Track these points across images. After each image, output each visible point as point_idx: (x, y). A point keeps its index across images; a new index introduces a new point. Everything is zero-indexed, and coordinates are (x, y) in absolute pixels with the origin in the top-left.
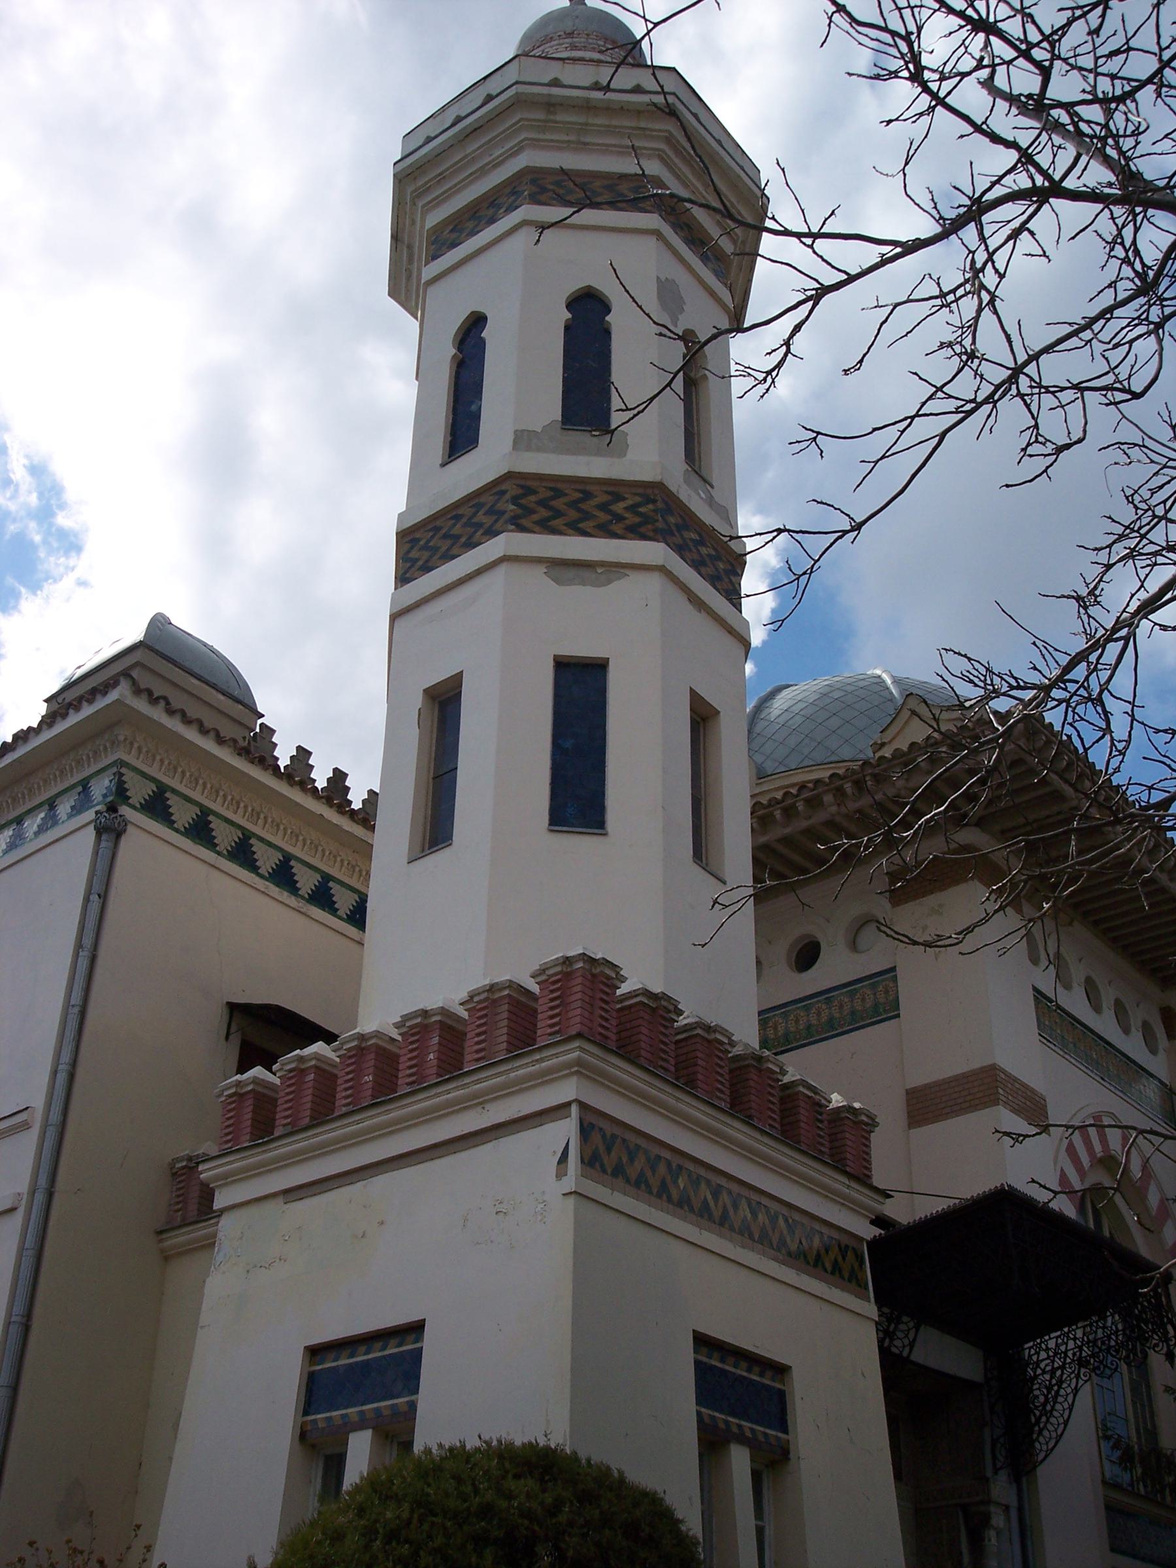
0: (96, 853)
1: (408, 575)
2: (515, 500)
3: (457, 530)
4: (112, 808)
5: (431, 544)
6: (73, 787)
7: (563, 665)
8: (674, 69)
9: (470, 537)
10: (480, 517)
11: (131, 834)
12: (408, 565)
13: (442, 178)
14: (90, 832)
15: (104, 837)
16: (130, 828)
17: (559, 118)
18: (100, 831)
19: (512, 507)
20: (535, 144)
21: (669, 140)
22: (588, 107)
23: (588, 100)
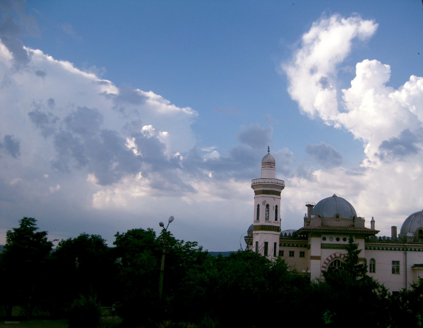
7: (275, 243)
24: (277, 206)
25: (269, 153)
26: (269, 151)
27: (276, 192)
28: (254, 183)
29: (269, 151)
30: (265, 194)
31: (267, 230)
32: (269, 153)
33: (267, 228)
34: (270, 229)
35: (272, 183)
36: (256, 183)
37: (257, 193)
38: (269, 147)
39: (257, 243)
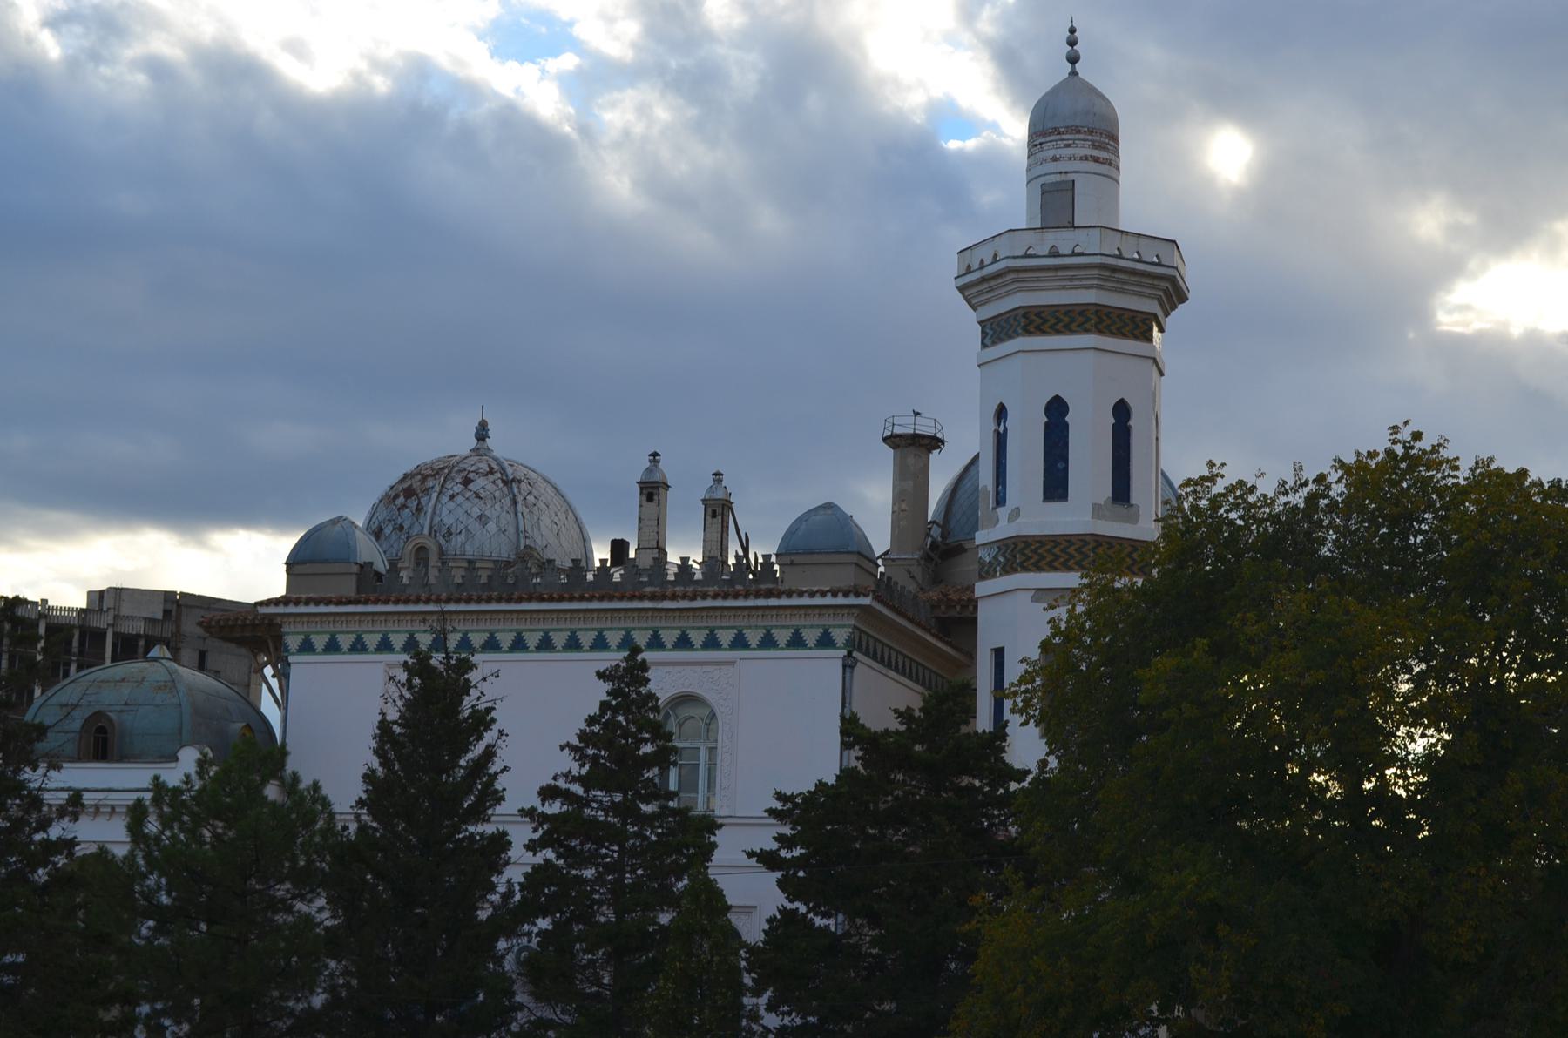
0: (844, 678)
1: (1025, 564)
2: (1093, 550)
3: (1056, 551)
4: (850, 654)
5: (1040, 551)
6: (818, 626)
8: (1175, 242)
9: (1068, 560)
10: (1071, 550)
11: (859, 668)
12: (1024, 558)
13: (1038, 280)
14: (840, 662)
15: (848, 670)
16: (859, 664)
17: (1116, 276)
18: (844, 667)
19: (1092, 554)
20: (1100, 288)
21: (1166, 292)
22: (1134, 272)
23: (1134, 269)
24: (1122, 411)
25: (1074, 73)
26: (1073, 59)
27: (1119, 316)
28: (969, 270)
29: (1073, 59)
30: (1040, 331)
31: (1056, 564)
32: (1074, 73)
33: (1056, 551)
34: (1078, 557)
35: (1081, 254)
36: (976, 265)
37: (994, 331)
38: (1072, 31)
39: (999, 653)
